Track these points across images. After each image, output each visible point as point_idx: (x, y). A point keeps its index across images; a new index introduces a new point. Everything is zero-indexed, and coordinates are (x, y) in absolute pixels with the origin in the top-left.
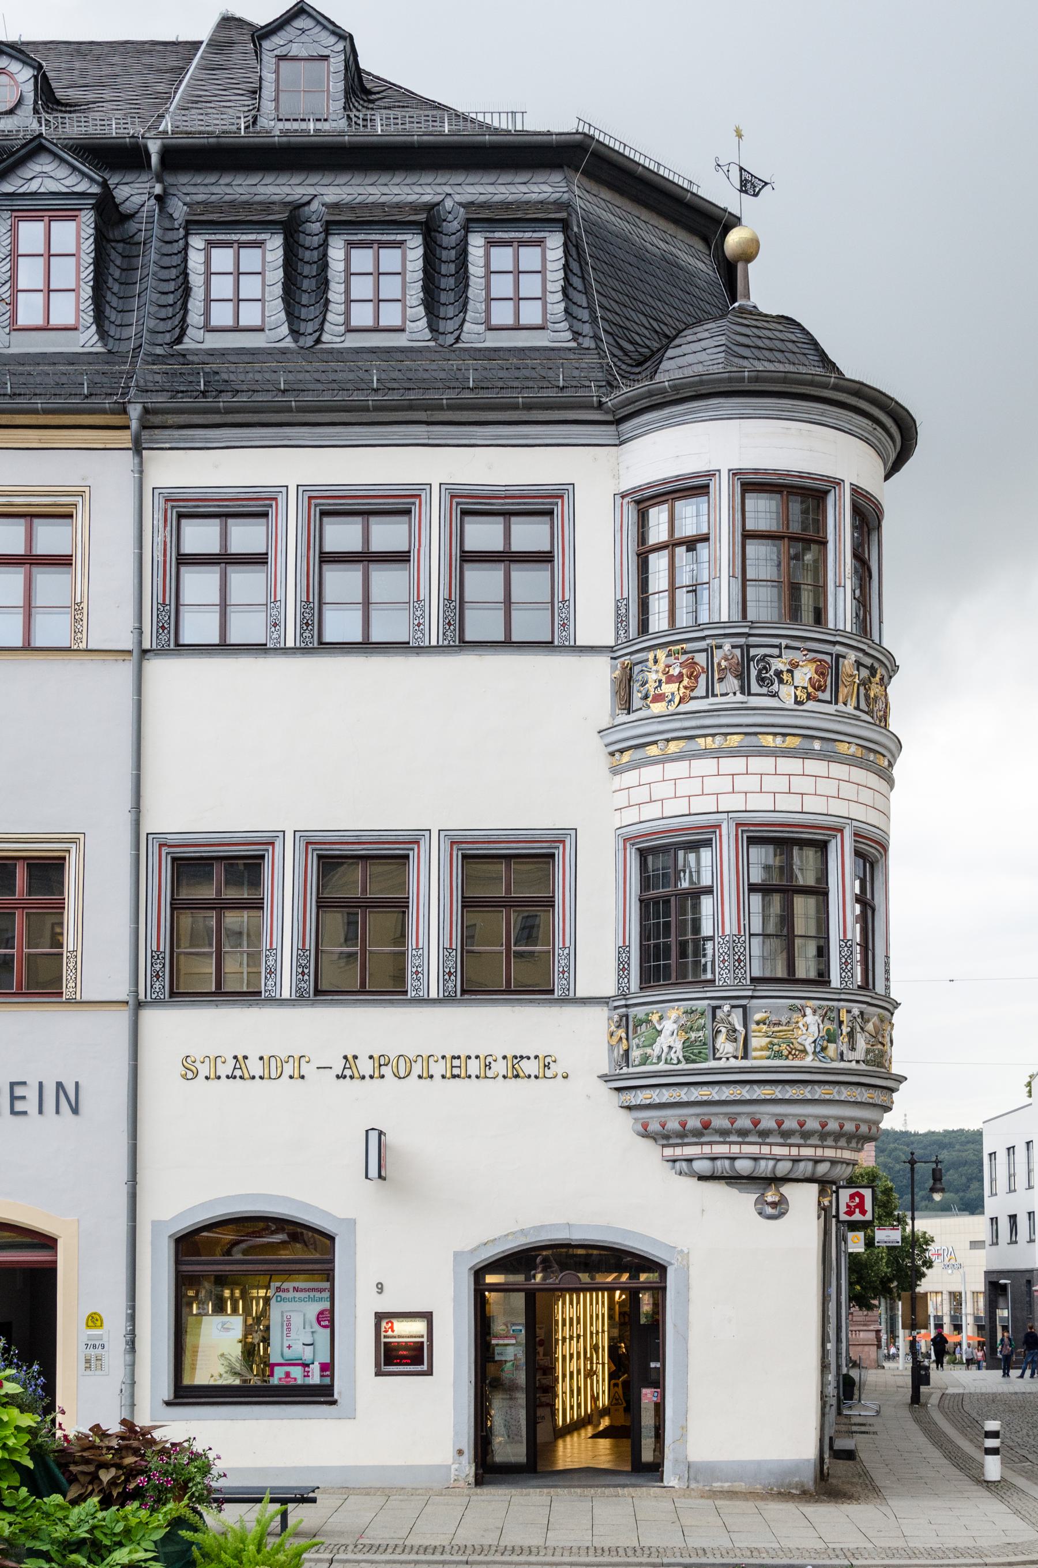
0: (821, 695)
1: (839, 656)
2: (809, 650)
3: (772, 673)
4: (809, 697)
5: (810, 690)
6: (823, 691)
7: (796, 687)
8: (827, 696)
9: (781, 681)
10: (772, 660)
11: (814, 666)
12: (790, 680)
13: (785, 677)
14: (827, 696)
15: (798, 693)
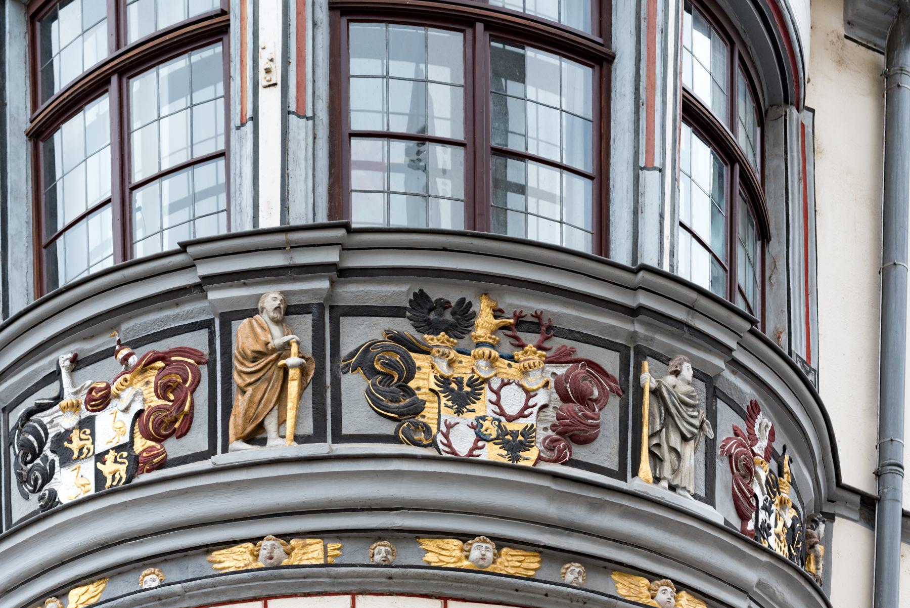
0: (174, 448)
1: (228, 318)
2: (136, 344)
3: (47, 450)
4: (136, 465)
5: (141, 444)
6: (183, 433)
7: (100, 458)
8: (197, 439)
9: (67, 458)
10: (44, 417)
11: (152, 376)
12: (88, 444)
13: (75, 446)
14: (197, 439)
15: (107, 469)
